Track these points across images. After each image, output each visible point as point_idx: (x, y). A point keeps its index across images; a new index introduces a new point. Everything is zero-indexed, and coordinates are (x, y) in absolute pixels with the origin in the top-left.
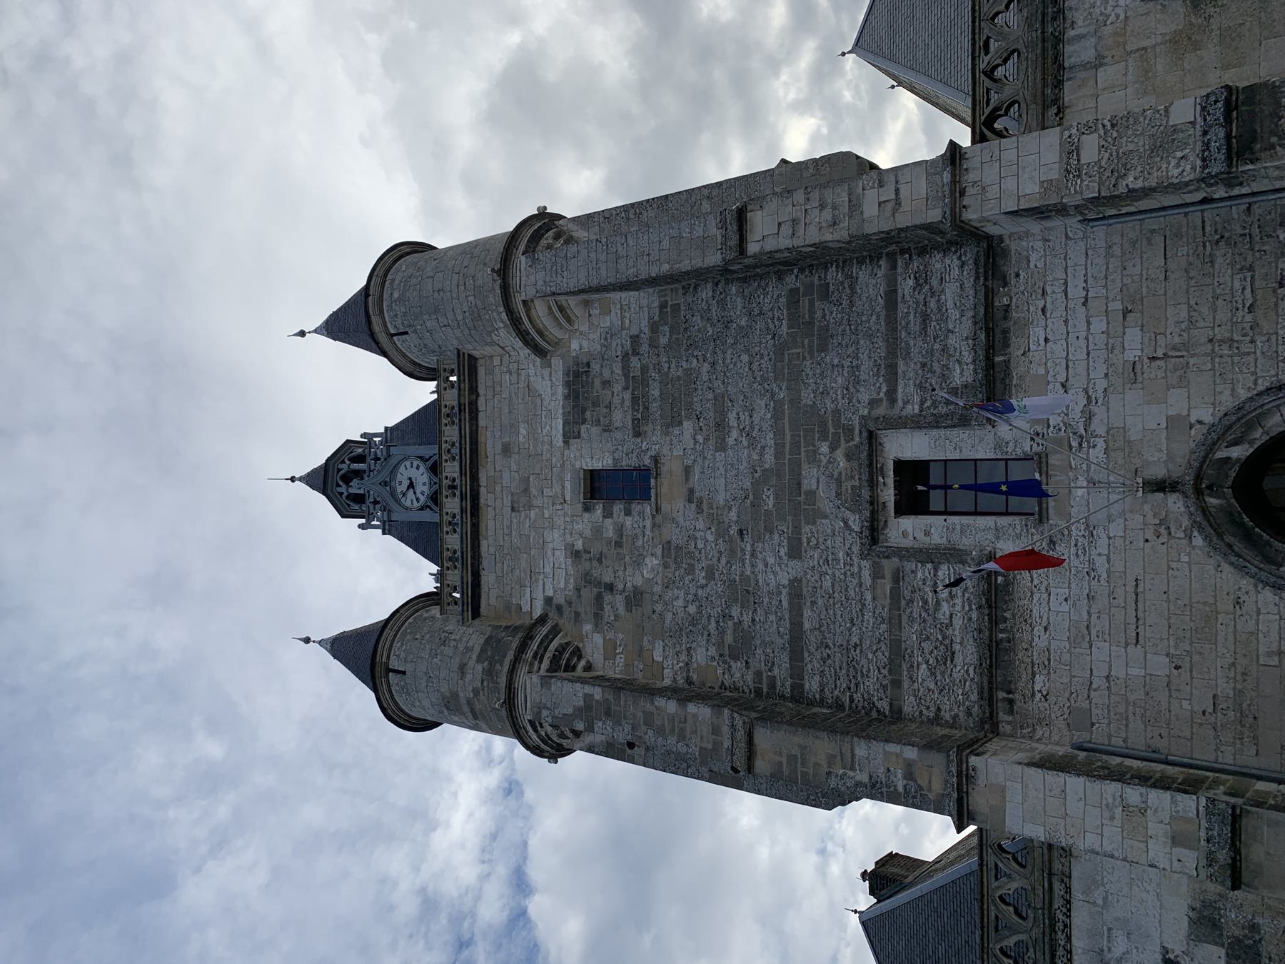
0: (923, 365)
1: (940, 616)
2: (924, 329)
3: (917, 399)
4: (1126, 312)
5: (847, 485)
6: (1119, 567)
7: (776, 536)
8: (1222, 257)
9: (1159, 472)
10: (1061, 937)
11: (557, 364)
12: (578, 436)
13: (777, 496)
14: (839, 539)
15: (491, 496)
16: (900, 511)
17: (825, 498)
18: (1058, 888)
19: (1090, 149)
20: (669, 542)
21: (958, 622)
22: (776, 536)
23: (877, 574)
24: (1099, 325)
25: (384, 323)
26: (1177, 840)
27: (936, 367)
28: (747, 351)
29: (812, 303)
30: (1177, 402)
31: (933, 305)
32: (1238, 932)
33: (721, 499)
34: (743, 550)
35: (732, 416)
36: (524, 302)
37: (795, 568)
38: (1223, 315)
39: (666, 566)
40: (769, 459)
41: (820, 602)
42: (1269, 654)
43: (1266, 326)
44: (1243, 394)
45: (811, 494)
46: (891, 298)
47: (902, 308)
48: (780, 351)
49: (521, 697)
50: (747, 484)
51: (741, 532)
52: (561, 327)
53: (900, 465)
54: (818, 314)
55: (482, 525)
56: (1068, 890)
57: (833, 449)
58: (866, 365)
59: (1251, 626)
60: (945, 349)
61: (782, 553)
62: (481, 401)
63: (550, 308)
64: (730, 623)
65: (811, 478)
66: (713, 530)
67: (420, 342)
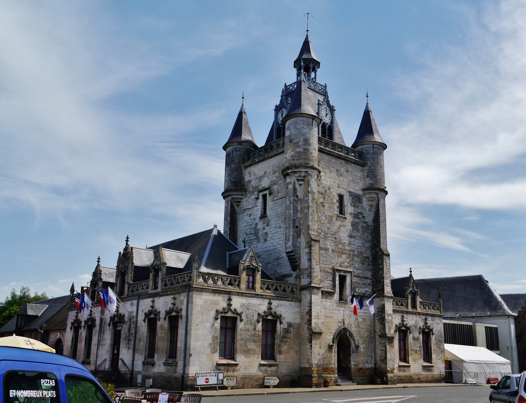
0: (358, 283)
1: (325, 281)
2: (363, 284)
3: (354, 281)
4: (363, 319)
5: (343, 265)
6: (334, 315)
7: (335, 247)
8: (368, 333)
9: (345, 323)
10: (283, 299)
11: (361, 193)
12: (350, 196)
13: (341, 248)
14: (335, 261)
15: (339, 163)
16: (339, 275)
17: (340, 260)
18: (290, 299)
19: (390, 318)
20: (333, 218)
21: (325, 284)
22: (335, 247)
23: (330, 268)
24: (362, 314)
25: (377, 145)
26: (315, 324)
27: (358, 285)
28: (362, 245)
29: (367, 262)
30: (353, 326)
31: (366, 286)
32: (290, 330)
33: (340, 234)
34: (332, 238)
35: (352, 240)
36: (378, 193)
37: (330, 250)
38: (363, 333)
39: (329, 216)
40: (346, 248)
41: (326, 255)
42: (325, 337)
43: (361, 339)
44: (354, 335)
45: (341, 256)
46: (367, 278)
47: (366, 280)
48: (361, 253)
49: (313, 171)
50: (343, 241)
51: (335, 238)
52: (369, 198)
53: (345, 277)
54: (366, 263)
55: (334, 158)
56: (290, 301)
57: (348, 262)
58: (359, 272)
59: (328, 335)
60: (360, 287)
61: (333, 248)
62: (355, 165)
63: (374, 198)
64: (321, 232)
65: (344, 256)
66: (335, 231)
67: (370, 153)
